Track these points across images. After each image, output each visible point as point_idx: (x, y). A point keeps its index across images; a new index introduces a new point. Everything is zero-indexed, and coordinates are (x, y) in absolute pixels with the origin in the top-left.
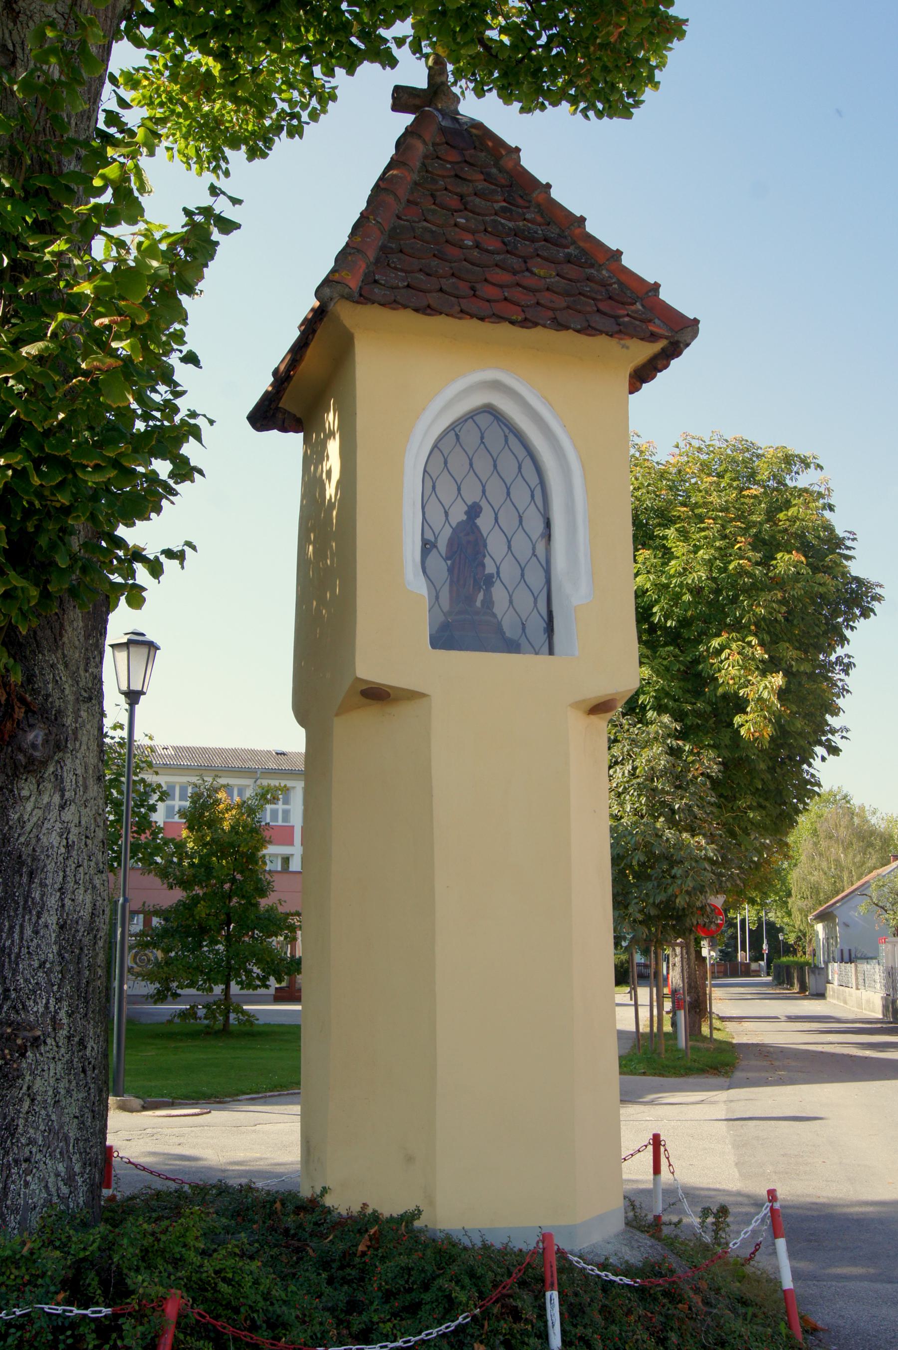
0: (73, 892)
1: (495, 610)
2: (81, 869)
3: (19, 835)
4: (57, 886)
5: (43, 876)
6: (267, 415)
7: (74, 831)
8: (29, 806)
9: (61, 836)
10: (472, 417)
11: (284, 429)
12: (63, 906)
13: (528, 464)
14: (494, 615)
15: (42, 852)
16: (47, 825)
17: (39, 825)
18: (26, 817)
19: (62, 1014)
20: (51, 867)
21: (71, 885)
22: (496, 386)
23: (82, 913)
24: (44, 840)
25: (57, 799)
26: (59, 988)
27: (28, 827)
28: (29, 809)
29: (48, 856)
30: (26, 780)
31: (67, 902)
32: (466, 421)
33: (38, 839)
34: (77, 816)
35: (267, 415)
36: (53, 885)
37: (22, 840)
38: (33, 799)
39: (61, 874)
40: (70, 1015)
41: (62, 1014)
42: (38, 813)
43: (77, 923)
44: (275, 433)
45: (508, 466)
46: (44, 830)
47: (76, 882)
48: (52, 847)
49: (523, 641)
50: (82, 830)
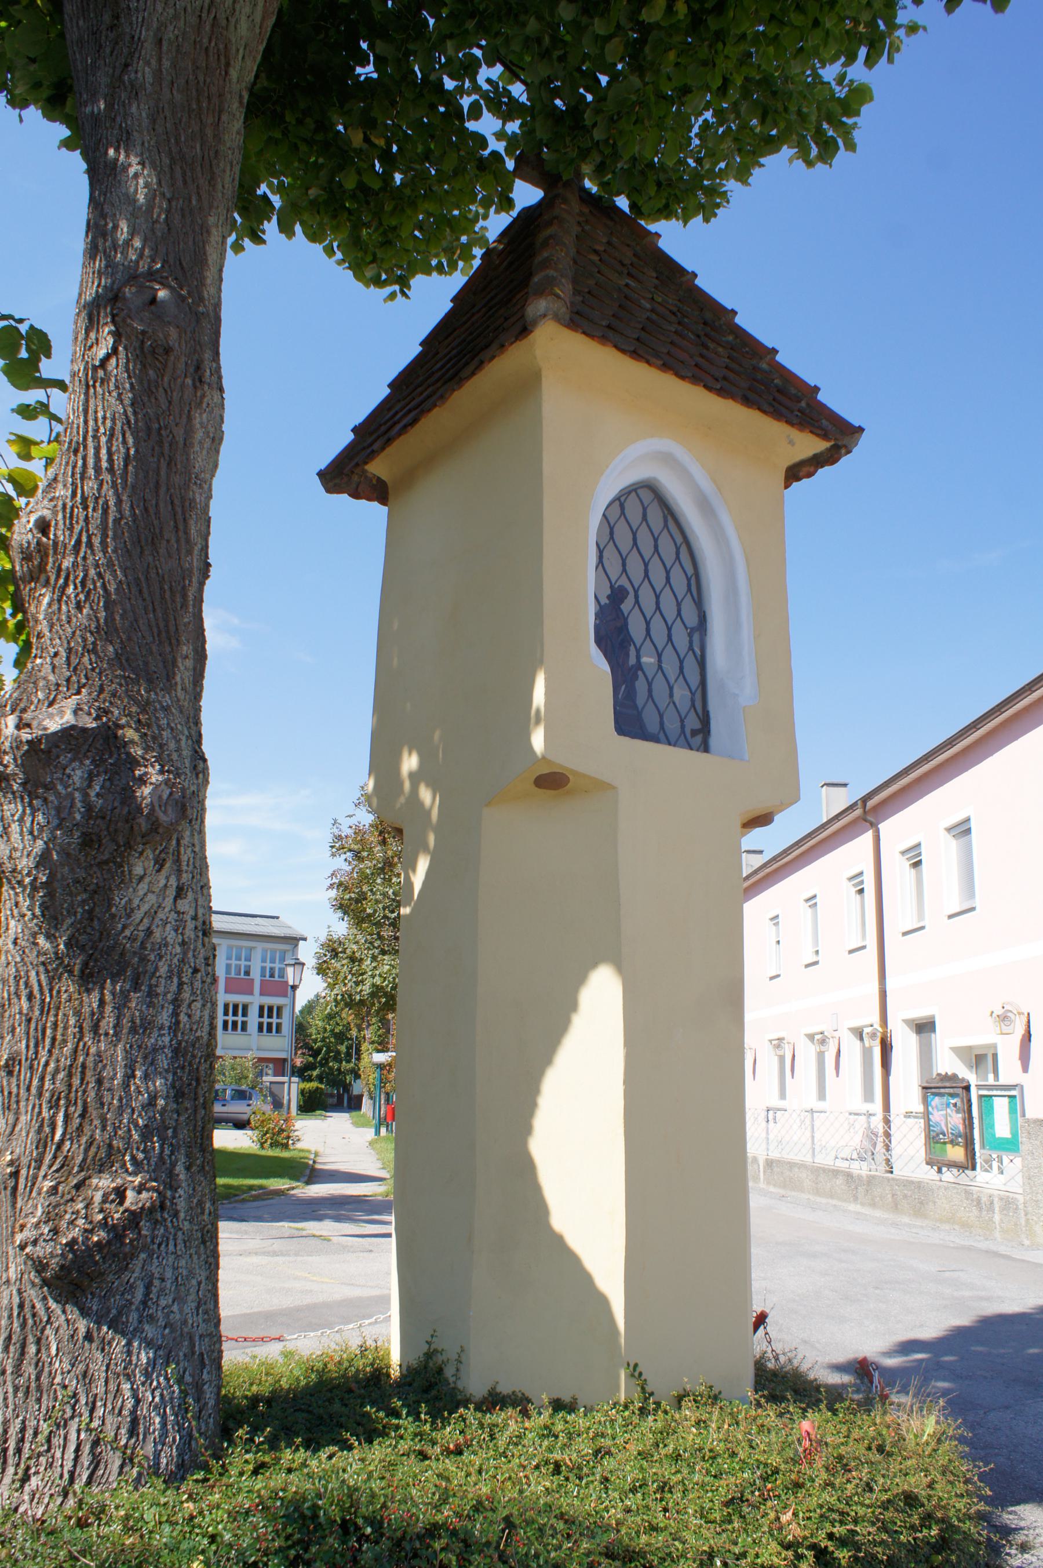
0: (189, 1006)
1: (638, 702)
2: (199, 975)
3: (124, 927)
4: (170, 997)
5: (154, 981)
6: (345, 474)
7: (191, 925)
8: (143, 887)
9: (176, 931)
10: (635, 490)
11: (356, 495)
12: (178, 1022)
13: (684, 550)
14: (636, 707)
15: (152, 950)
16: (161, 915)
17: (152, 914)
18: (136, 902)
19: (180, 1169)
20: (163, 970)
21: (186, 995)
22: (667, 459)
23: (199, 1034)
24: (157, 934)
25: (173, 882)
26: (175, 1132)
27: (138, 915)
28: (141, 893)
29: (161, 957)
30: (141, 853)
31: (183, 1018)
32: (630, 493)
33: (149, 932)
34: (193, 905)
35: (345, 474)
36: (165, 995)
37: (127, 933)
38: (147, 880)
39: (175, 980)
40: (188, 1168)
41: (180, 1169)
42: (152, 899)
43: (194, 1046)
44: (345, 497)
45: (667, 549)
46: (157, 921)
47: (193, 993)
48: (166, 945)
49: (662, 736)
50: (199, 924)
